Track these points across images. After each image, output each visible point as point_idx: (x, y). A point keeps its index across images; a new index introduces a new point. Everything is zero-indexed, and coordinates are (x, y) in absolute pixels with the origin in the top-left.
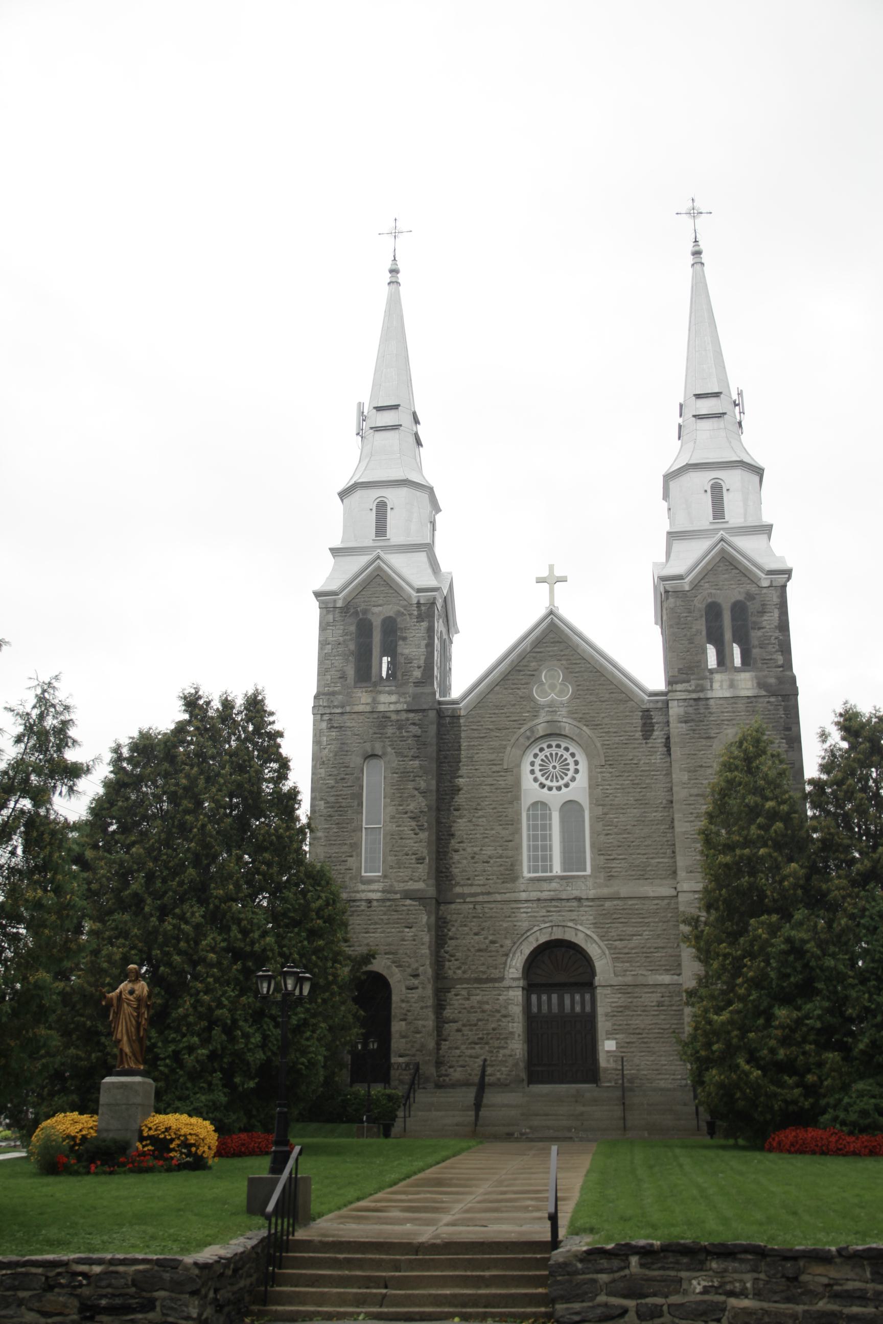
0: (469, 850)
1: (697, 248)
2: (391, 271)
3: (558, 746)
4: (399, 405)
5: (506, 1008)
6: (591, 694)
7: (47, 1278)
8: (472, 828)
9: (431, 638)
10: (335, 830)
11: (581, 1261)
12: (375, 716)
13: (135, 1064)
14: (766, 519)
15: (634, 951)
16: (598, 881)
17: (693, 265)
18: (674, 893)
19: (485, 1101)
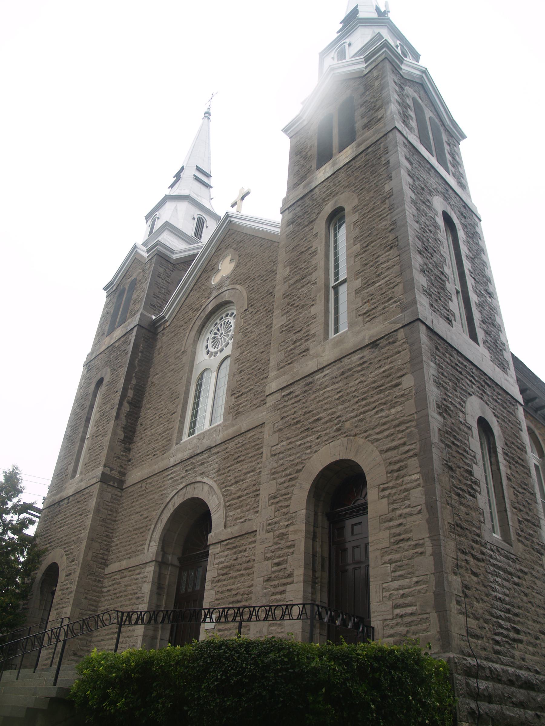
3: (227, 315)
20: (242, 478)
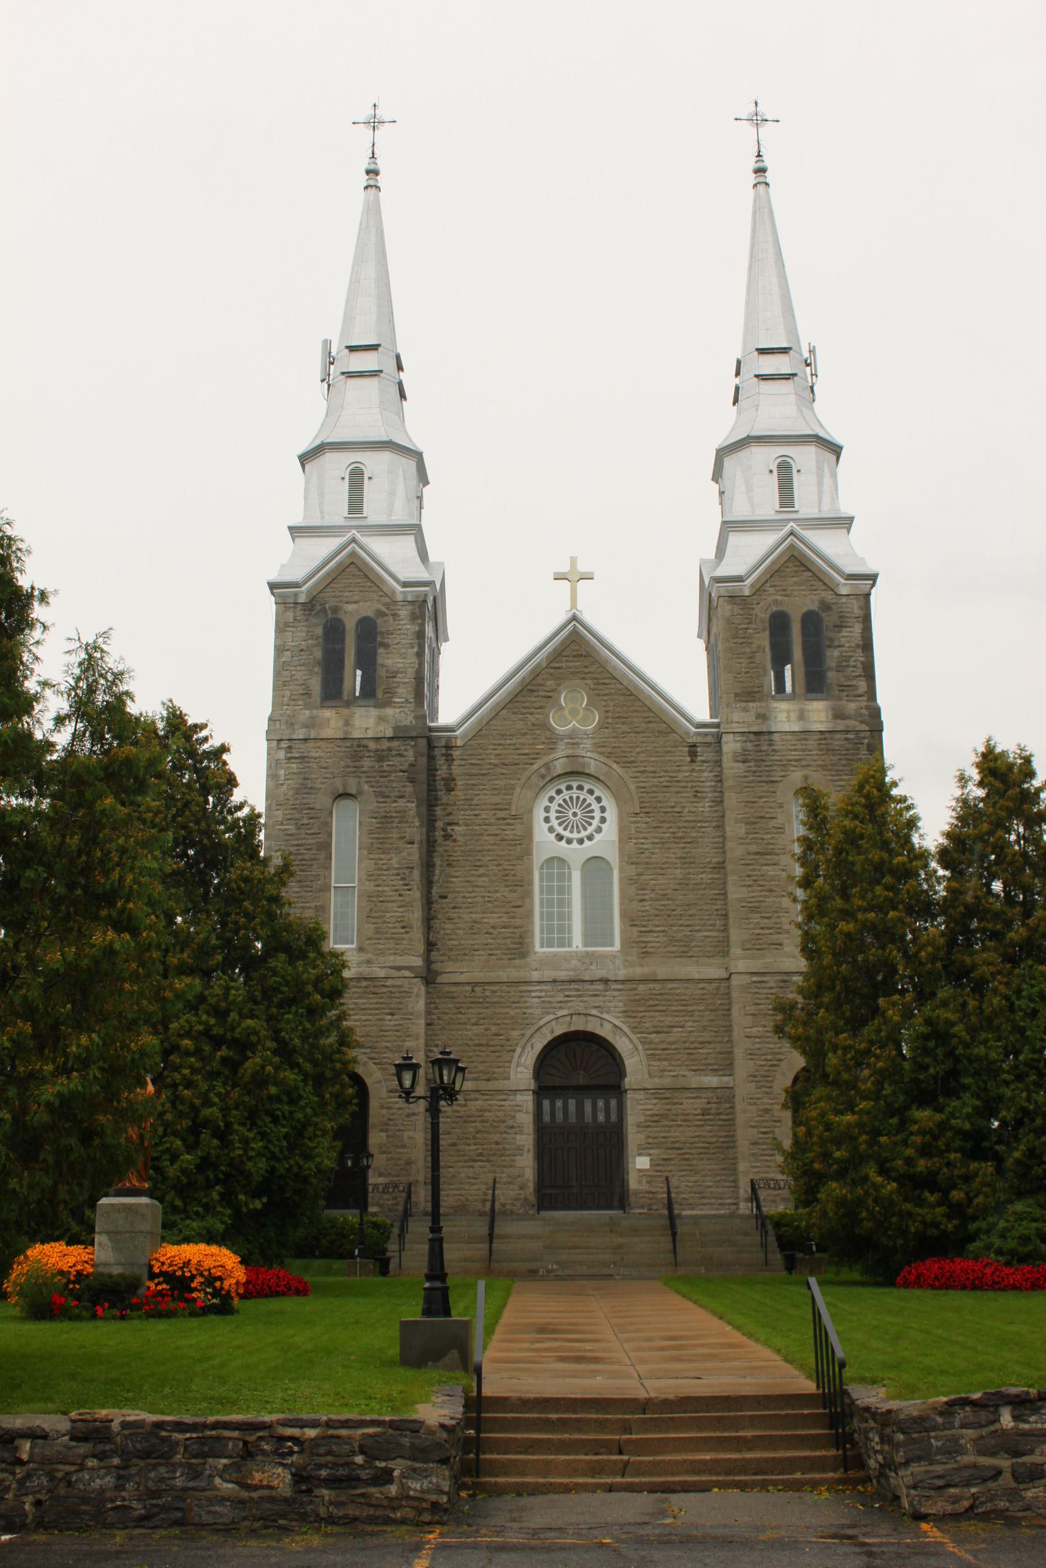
0: (466, 916)
1: (760, 165)
2: (368, 172)
3: (580, 788)
4: (379, 345)
5: (514, 1117)
6: (623, 723)
7: (245, 1443)
8: (471, 889)
9: (421, 647)
10: (297, 890)
11: (941, 1414)
12: (348, 744)
13: (138, 1181)
14: (845, 509)
15: (673, 1047)
16: (629, 958)
17: (755, 185)
18: (722, 974)
19: (497, 1231)
20: (666, 1030)
